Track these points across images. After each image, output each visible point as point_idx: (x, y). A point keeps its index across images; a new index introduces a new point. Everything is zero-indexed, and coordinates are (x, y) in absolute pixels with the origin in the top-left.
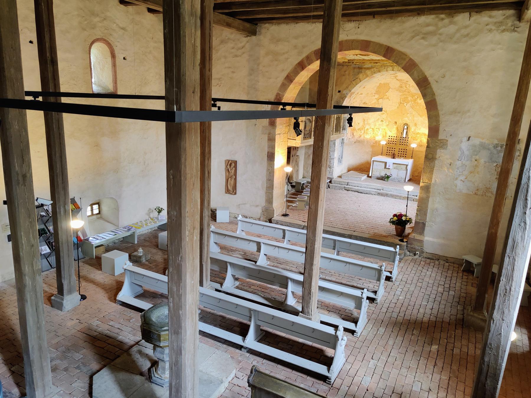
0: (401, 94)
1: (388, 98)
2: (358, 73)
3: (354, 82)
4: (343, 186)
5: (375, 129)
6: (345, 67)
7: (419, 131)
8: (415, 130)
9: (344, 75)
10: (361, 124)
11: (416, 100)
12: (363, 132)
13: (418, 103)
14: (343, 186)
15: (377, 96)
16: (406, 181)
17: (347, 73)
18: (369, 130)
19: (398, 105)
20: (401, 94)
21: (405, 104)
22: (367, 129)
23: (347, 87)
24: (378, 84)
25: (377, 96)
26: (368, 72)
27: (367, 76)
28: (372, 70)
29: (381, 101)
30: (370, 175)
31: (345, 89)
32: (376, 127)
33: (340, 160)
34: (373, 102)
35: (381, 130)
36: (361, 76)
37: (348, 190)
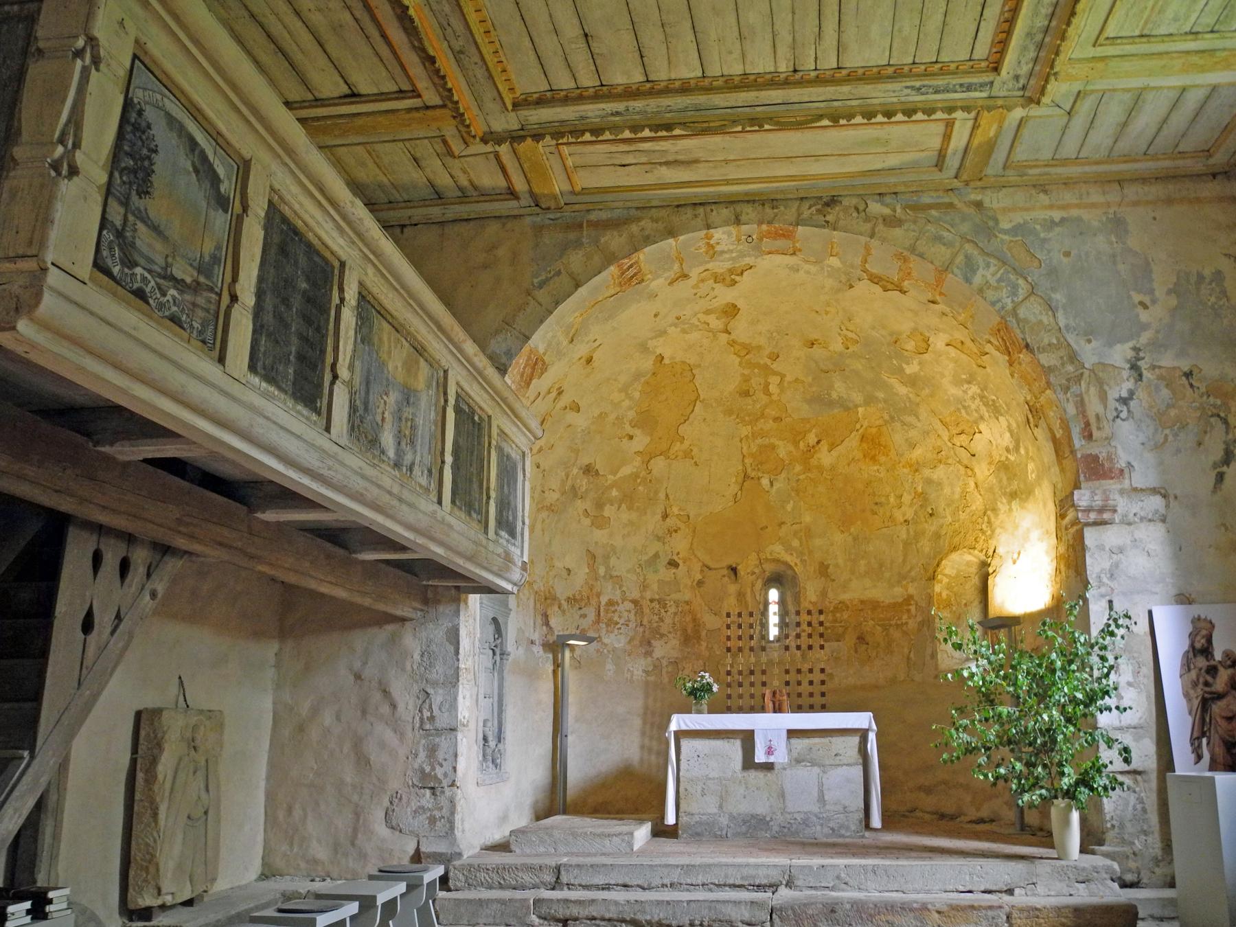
0: (745, 431)
1: (688, 454)
2: (564, 248)
3: (542, 295)
5: (646, 603)
6: (493, 228)
7: (845, 597)
8: (824, 594)
9: (485, 266)
10: (582, 573)
11: (811, 450)
12: (592, 616)
13: (820, 468)
14: (530, 895)
15: (641, 441)
16: (876, 822)
17: (502, 252)
18: (621, 608)
19: (735, 488)
20: (745, 431)
21: (765, 482)
22: (611, 603)
23: (508, 323)
24: (648, 364)
25: (641, 441)
26: (615, 241)
27: (610, 259)
28: (634, 228)
29: (659, 464)
30: (671, 819)
32: (648, 595)
33: (492, 754)
34: (626, 471)
35: (672, 610)
36: (575, 260)
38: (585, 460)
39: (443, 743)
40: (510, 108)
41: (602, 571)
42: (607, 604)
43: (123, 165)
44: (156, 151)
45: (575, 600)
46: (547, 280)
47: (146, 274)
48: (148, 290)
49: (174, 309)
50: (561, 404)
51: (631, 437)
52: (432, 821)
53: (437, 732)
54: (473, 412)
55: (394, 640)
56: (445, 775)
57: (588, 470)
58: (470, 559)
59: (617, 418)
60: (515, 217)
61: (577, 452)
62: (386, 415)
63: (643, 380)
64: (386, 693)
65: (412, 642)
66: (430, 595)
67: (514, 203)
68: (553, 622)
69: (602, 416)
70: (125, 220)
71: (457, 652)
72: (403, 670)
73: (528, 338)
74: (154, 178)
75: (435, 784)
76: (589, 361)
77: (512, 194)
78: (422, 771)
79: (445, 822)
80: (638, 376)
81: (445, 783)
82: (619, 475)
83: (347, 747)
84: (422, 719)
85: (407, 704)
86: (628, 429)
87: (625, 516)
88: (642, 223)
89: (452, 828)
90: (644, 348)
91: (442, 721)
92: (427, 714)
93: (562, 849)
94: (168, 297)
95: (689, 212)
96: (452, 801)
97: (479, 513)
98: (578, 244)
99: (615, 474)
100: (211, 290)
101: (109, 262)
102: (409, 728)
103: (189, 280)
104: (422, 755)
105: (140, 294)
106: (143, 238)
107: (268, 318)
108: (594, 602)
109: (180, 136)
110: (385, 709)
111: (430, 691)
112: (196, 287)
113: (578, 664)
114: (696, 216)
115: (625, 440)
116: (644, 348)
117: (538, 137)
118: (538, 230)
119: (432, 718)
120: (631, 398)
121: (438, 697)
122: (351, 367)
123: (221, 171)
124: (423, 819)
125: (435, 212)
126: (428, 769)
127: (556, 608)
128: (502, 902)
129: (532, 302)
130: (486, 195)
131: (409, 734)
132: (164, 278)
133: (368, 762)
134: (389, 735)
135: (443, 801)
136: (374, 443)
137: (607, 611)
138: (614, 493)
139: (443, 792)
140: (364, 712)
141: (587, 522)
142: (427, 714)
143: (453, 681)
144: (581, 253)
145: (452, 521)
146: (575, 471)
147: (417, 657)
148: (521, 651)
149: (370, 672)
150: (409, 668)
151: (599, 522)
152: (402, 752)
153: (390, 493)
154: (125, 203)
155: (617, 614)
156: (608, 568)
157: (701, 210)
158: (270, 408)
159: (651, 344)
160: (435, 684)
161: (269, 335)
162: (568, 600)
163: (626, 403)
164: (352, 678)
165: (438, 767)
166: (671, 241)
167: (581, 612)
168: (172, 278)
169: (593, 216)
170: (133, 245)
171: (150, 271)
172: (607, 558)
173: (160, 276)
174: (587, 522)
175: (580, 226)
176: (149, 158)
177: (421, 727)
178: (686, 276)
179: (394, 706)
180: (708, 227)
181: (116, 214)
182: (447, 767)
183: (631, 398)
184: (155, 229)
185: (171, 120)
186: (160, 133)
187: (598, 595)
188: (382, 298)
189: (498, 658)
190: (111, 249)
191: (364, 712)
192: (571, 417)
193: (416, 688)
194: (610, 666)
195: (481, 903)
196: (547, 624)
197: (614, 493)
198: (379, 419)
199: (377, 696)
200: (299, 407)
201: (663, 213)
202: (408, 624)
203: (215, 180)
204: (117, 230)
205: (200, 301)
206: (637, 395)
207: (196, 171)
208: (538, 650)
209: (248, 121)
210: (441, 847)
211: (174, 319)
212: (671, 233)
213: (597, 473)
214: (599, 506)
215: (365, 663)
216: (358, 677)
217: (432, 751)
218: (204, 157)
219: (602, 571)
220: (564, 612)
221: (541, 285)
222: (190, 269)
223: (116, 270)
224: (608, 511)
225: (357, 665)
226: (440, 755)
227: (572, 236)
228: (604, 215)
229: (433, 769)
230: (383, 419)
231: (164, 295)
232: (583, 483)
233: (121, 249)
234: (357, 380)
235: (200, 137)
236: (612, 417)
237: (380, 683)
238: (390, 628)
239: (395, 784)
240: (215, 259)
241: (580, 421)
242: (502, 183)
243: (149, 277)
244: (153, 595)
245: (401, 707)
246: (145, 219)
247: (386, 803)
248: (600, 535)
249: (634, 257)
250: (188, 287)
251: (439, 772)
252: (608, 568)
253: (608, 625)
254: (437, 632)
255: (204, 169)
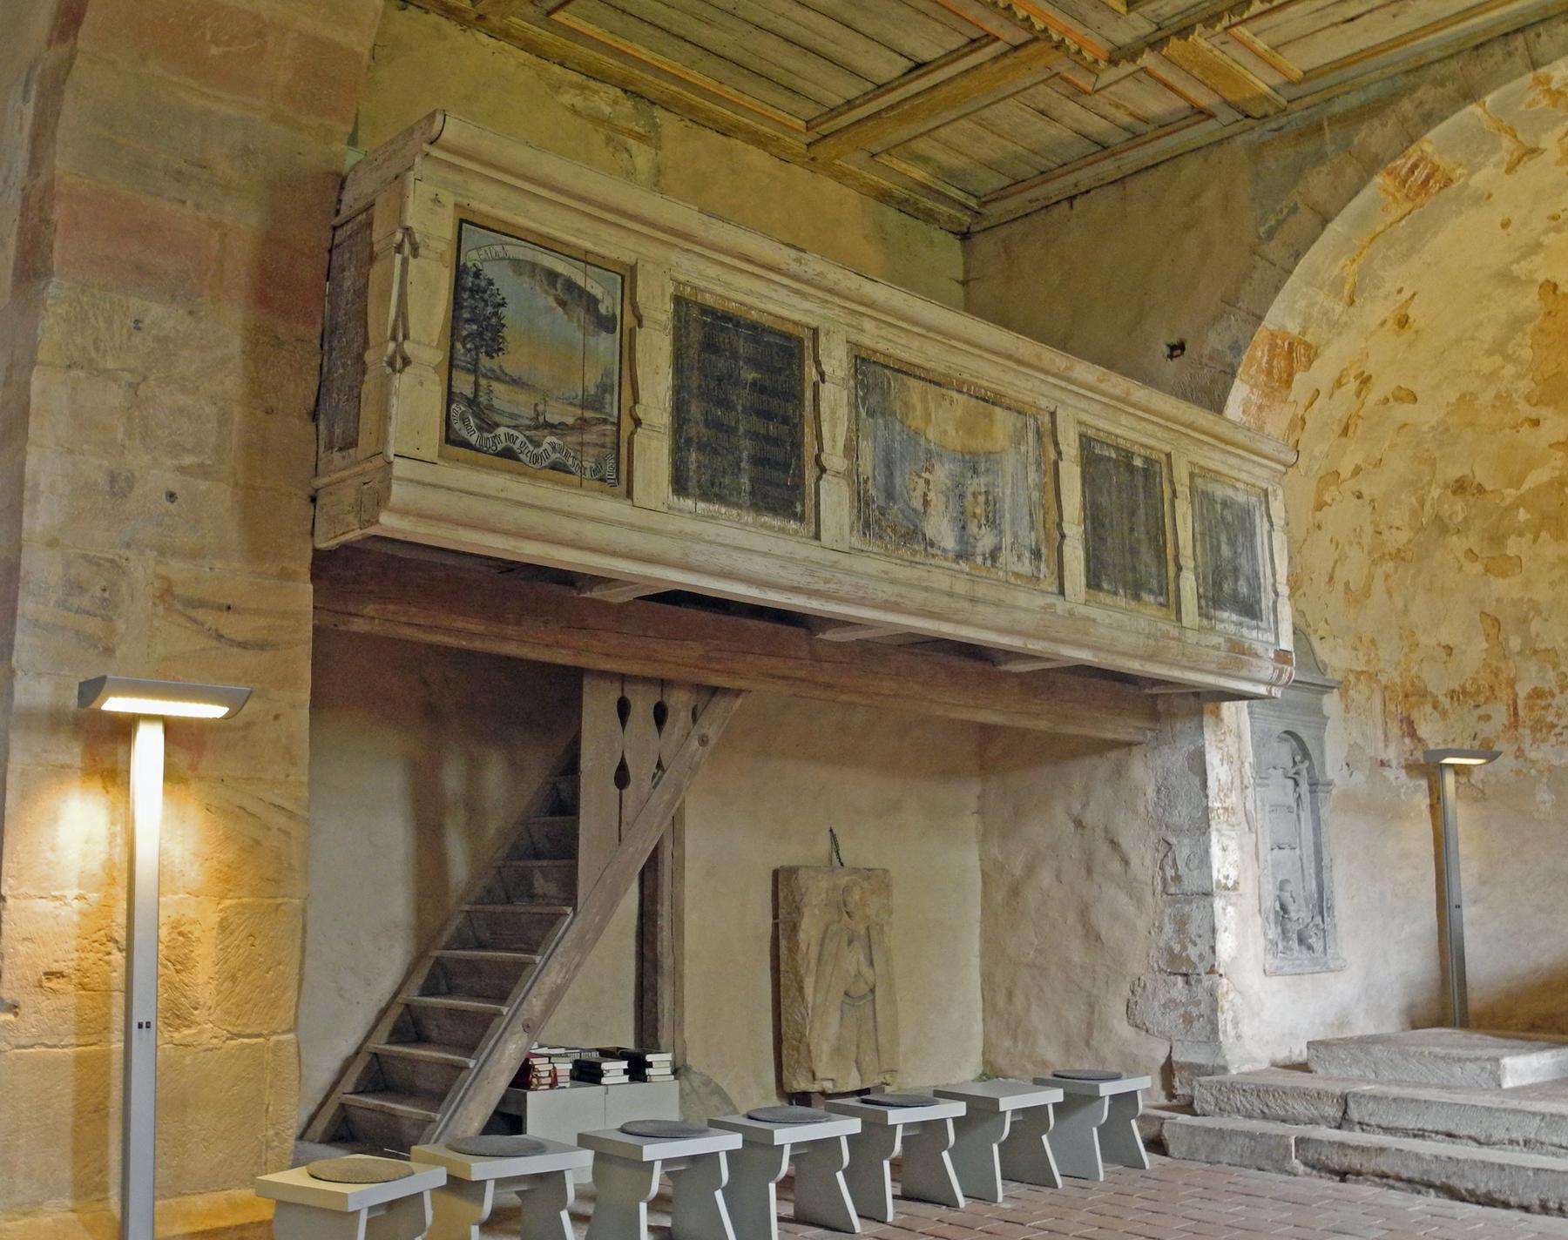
2: (1297, 172)
3: (1274, 250)
4: (1293, 1132)
6: (1191, 169)
9: (1187, 227)
10: (1474, 652)
12: (1501, 714)
17: (1209, 199)
22: (1537, 694)
23: (1230, 301)
24: (1530, 300)
26: (1375, 136)
28: (1406, 106)
31: (1216, 319)
34: (1538, 477)
36: (1318, 184)
37: (1343, 1175)
38: (1454, 473)
39: (1195, 912)
40: (1123, 9)
41: (1515, 643)
42: (1530, 697)
43: (465, 333)
44: (503, 305)
45: (1465, 693)
46: (1280, 223)
47: (512, 432)
48: (515, 447)
49: (554, 456)
50: (1374, 395)
51: (1536, 423)
52: (1188, 1020)
53: (1189, 898)
54: (1129, 455)
55: (1119, 772)
56: (1201, 957)
57: (1460, 487)
58: (1151, 658)
59: (1498, 397)
60: (1221, 142)
61: (1433, 463)
62: (931, 496)
63: (1529, 327)
64: (1114, 844)
65: (1143, 773)
66: (1161, 707)
67: (1211, 125)
68: (1423, 731)
69: (1467, 399)
70: (477, 385)
71: (1204, 786)
72: (1135, 812)
73: (1260, 318)
74: (505, 332)
75: (1190, 967)
76: (1403, 322)
77: (1203, 114)
78: (1170, 951)
79: (1204, 1020)
80: (1516, 323)
81: (1201, 969)
82: (1525, 487)
83: (1072, 917)
84: (1164, 880)
85: (1143, 859)
86: (1525, 410)
87: (1549, 549)
88: (1419, 93)
89: (1215, 1031)
90: (1506, 278)
91: (1191, 882)
92: (1170, 872)
93: (1386, 1073)
94: (545, 446)
95: (1498, 51)
96: (1212, 994)
97: (1162, 590)
98: (1320, 157)
99: (1518, 484)
100: (605, 421)
101: (464, 433)
102: (1149, 891)
103: (570, 421)
104: (1169, 929)
105: (508, 454)
106: (502, 397)
107: (696, 429)
108: (1504, 694)
109: (533, 277)
110: (1115, 866)
111: (1173, 840)
112: (583, 425)
113: (1478, 796)
114: (1510, 54)
115: (1525, 429)
116: (1506, 278)
117: (1184, 32)
118: (1257, 151)
119: (1177, 878)
120: (1516, 361)
121: (1183, 850)
122: (851, 451)
123: (597, 291)
124: (1175, 1016)
125: (1108, 168)
126: (1177, 949)
127: (1428, 708)
128: (1251, 1136)
129: (1261, 263)
130: (1166, 126)
131: (1149, 899)
132: (536, 428)
133: (1098, 938)
134: (1123, 900)
135: (1201, 993)
136: (912, 535)
137: (1531, 709)
138: (1522, 515)
139: (1199, 981)
140: (1089, 871)
141: (1478, 567)
142: (1170, 872)
143: (1202, 825)
144: (1325, 169)
145: (1093, 612)
146: (1435, 492)
147: (1151, 794)
148: (1359, 777)
149: (1092, 816)
150: (1142, 809)
151: (1500, 566)
152: (1142, 924)
153: (950, 595)
154: (474, 369)
155: (1552, 711)
156: (1527, 639)
157: (1519, 41)
158: (710, 530)
159: (1516, 269)
160: (1178, 831)
161: (701, 448)
162: (1452, 694)
163: (1510, 370)
164: (1071, 826)
165: (1190, 946)
166: (1473, 108)
167: (1480, 711)
168: (548, 425)
169: (1338, 107)
170: (490, 407)
171: (515, 427)
172: (1523, 621)
173: (529, 428)
174: (1478, 567)
175: (1320, 128)
176: (496, 314)
177: (1165, 891)
178: (1534, 151)
179: (1126, 862)
180: (1535, 65)
181: (464, 384)
182: (1203, 947)
183: (1516, 361)
184: (515, 382)
185: (517, 264)
186: (505, 282)
187: (1512, 683)
188: (898, 352)
189: (1304, 788)
190: (463, 419)
191: (1089, 871)
192: (1402, 412)
193: (1153, 838)
194: (1544, 796)
195: (1221, 1134)
196: (1413, 734)
197: (1522, 515)
198: (917, 504)
199: (1105, 848)
200: (765, 519)
201: (1454, 65)
202: (1136, 750)
203: (592, 303)
204: (469, 400)
205: (588, 437)
206: (1527, 353)
207: (562, 304)
208: (1396, 775)
209: (620, 226)
210: (1199, 1056)
211: (554, 467)
212: (1469, 95)
213: (1480, 489)
214: (1496, 539)
215: (1085, 805)
216: (1079, 824)
217: (1181, 923)
218: (570, 286)
219: (1515, 643)
220: (1444, 714)
221: (1271, 234)
222: (571, 409)
223: (473, 439)
224: (1513, 546)
225: (1077, 808)
226: (1193, 929)
227: (1309, 147)
228: (1354, 100)
229: (1184, 948)
230: (926, 503)
231: (538, 444)
232: (1457, 509)
233: (475, 415)
234: (867, 464)
235: (561, 266)
236: (1488, 396)
237: (1106, 830)
238: (1113, 755)
239: (1136, 967)
240: (605, 388)
241: (1425, 415)
242: (1181, 103)
243: (516, 433)
244: (703, 741)
245: (1135, 861)
246: (500, 377)
247: (1127, 993)
248: (1500, 586)
249: (1414, 153)
250: (572, 428)
251: (1193, 953)
252: (1527, 639)
253: (1534, 730)
254: (1174, 758)
255: (573, 296)
